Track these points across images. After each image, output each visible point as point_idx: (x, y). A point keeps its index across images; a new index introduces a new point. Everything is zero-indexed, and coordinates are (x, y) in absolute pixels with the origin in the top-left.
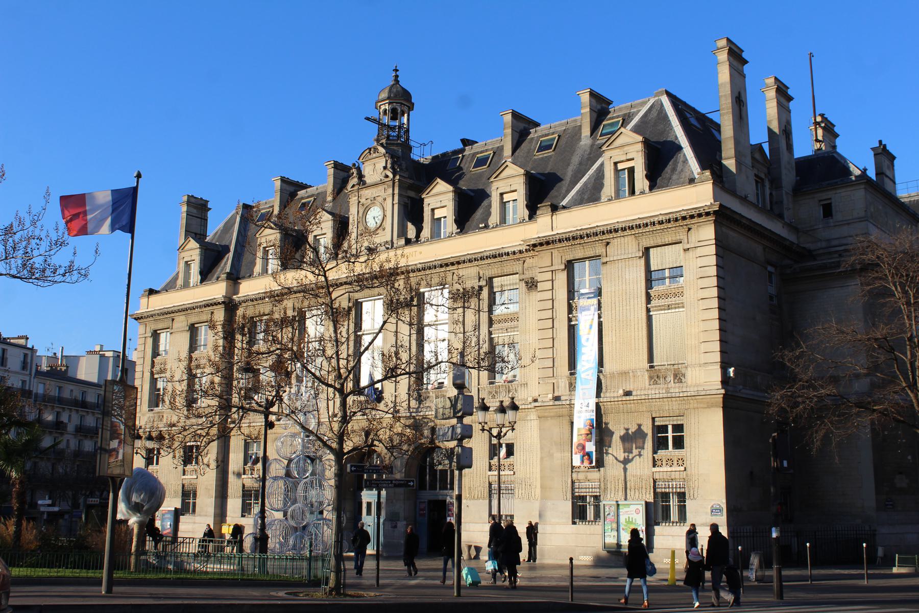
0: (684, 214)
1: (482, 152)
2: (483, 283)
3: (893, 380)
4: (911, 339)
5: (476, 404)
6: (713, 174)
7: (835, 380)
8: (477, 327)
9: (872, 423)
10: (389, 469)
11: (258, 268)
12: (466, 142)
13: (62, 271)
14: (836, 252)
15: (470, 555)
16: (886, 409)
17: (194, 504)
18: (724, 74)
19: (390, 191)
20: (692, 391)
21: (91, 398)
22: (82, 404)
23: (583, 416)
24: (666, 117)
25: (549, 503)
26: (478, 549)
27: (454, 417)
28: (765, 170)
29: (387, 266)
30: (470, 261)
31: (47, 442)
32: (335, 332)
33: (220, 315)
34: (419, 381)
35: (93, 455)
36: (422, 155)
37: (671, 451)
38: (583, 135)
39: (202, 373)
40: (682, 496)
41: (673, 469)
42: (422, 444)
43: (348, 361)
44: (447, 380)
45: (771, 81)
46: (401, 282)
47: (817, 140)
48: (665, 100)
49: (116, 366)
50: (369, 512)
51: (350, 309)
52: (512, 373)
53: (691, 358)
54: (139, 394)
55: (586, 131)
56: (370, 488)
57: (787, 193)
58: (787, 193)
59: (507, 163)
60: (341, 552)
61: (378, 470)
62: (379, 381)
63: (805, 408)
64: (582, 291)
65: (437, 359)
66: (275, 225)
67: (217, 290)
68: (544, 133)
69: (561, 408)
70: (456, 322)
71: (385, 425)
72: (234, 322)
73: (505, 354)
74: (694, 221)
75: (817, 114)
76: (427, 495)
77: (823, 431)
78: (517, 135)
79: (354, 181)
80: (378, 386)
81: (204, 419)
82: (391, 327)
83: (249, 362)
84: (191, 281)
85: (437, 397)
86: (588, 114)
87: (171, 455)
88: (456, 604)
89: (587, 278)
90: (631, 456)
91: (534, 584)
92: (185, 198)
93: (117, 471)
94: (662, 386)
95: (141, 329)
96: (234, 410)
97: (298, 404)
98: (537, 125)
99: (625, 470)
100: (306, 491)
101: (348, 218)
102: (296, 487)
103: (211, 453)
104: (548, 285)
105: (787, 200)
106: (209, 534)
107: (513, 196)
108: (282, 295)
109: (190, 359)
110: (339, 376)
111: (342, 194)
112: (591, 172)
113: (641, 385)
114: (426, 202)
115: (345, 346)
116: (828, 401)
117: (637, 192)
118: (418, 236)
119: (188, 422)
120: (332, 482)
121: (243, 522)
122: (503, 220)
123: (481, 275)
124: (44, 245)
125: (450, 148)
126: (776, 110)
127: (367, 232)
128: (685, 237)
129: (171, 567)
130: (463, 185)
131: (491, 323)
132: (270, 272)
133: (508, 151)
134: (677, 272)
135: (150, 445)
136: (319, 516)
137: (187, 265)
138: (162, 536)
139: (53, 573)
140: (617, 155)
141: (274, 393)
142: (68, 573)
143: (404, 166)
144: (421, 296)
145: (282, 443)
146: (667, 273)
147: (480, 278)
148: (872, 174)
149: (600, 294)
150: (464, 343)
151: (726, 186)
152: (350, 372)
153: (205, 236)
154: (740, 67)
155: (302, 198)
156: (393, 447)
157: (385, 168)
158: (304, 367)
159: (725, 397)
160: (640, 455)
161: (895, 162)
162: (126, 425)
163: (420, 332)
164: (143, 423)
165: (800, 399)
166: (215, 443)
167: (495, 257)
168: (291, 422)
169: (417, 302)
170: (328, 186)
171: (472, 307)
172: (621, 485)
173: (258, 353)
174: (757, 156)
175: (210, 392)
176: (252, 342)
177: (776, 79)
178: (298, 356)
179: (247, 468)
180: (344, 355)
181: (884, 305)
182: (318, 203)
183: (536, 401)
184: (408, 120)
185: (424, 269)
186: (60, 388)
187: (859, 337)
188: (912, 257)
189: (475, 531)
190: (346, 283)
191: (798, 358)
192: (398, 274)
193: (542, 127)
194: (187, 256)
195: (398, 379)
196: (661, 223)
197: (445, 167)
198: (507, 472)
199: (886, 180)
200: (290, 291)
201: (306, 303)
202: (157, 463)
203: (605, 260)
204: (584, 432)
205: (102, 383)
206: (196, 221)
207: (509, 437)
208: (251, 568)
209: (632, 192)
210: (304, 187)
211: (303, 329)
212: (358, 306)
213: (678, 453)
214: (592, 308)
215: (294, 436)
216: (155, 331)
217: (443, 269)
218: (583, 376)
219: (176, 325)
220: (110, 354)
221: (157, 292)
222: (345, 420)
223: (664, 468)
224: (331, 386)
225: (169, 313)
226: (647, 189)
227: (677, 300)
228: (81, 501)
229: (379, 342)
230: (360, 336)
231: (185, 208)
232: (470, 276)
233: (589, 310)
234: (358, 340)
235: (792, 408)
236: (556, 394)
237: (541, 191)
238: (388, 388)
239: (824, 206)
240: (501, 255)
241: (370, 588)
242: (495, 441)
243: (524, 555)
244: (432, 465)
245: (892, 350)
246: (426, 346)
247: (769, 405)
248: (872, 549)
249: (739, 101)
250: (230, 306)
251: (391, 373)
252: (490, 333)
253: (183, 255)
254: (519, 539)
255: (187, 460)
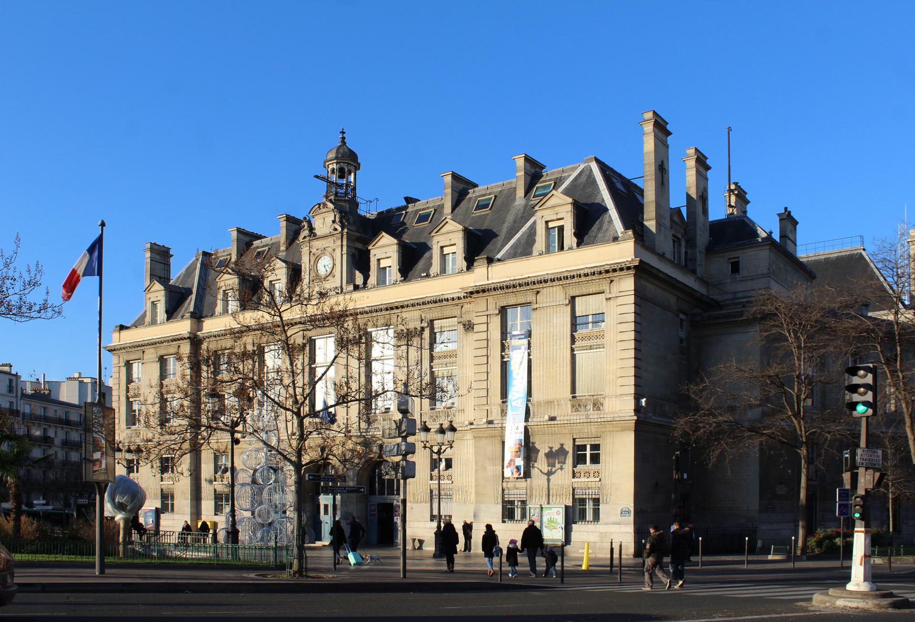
0: (607, 268)
1: (423, 209)
2: (425, 324)
3: (781, 409)
4: (799, 377)
5: (418, 426)
6: (635, 233)
7: (732, 409)
8: (419, 362)
9: (761, 444)
10: (343, 478)
11: (219, 308)
12: (409, 200)
13: (37, 308)
14: (740, 303)
15: (414, 546)
16: (773, 433)
17: (173, 505)
18: (649, 144)
19: (339, 242)
20: (609, 417)
21: (74, 417)
22: (67, 422)
23: (514, 436)
24: (594, 182)
25: (483, 506)
26: (421, 542)
27: (399, 436)
28: (682, 231)
29: (336, 309)
30: (413, 305)
31: (37, 453)
32: (291, 364)
33: (186, 348)
34: (368, 406)
35: (78, 465)
36: (369, 210)
37: (588, 466)
38: (517, 196)
39: (173, 398)
40: (597, 501)
41: (590, 480)
42: (371, 458)
43: (304, 389)
44: (393, 406)
45: (691, 151)
46: (350, 323)
47: (730, 206)
48: (594, 167)
49: (94, 390)
50: (326, 512)
51: (304, 345)
52: (451, 401)
53: (608, 390)
54: (117, 415)
55: (520, 193)
56: (326, 493)
57: (700, 252)
58: (700, 252)
59: (447, 220)
60: (304, 542)
61: (333, 479)
62: (332, 406)
63: (705, 432)
64: (514, 333)
65: (383, 389)
66: (233, 270)
67: (183, 327)
68: (481, 193)
69: (493, 430)
70: (400, 358)
71: (337, 442)
72: (198, 354)
73: (445, 385)
74: (616, 274)
75: (732, 181)
76: (377, 499)
77: (717, 452)
78: (456, 195)
79: (305, 233)
80: (332, 410)
81: (176, 436)
82: (342, 361)
83: (214, 388)
84: (158, 318)
85: (384, 420)
86: (523, 177)
87: (149, 465)
88: (402, 584)
89: (519, 322)
90: (554, 470)
91: (468, 569)
92: (149, 246)
93: (102, 478)
94: (582, 413)
95: (115, 360)
96: (203, 428)
97: (260, 424)
98: (475, 186)
99: (549, 480)
100: (270, 494)
101: (301, 266)
102: (262, 492)
103: (185, 464)
104: (484, 327)
105: (700, 258)
106: (187, 528)
107: (453, 249)
108: (242, 332)
109: (161, 386)
110: (296, 402)
111: (294, 244)
112: (524, 229)
113: (564, 412)
114: (372, 253)
115: (300, 376)
116: (725, 426)
117: (566, 247)
118: (365, 283)
119: (162, 438)
120: (293, 488)
121: (216, 519)
122: (443, 270)
124: (18, 286)
125: (394, 205)
126: (694, 178)
127: (318, 278)
128: (608, 288)
129: (155, 554)
130: (407, 238)
131: (432, 358)
132: (230, 312)
133: (448, 208)
134: (599, 318)
135: (129, 456)
136: (283, 515)
137: (154, 304)
138: (145, 530)
139: (52, 558)
140: (548, 215)
141: (238, 415)
142: (65, 558)
143: (351, 220)
144: (368, 335)
145: (248, 456)
146: (590, 319)
147: (422, 320)
148: (776, 236)
149: (530, 336)
150: (408, 375)
151: (647, 244)
152: (305, 399)
153: (168, 279)
154: (664, 138)
155: (258, 247)
156: (346, 460)
157: (334, 222)
158: (264, 394)
159: (638, 424)
160: (562, 469)
161: (798, 226)
162: (106, 441)
163: (368, 366)
164: (121, 439)
165: (701, 425)
166: (188, 456)
167: (435, 302)
168: (254, 439)
169: (364, 340)
170: (281, 235)
171: (415, 344)
172: (545, 492)
173: (222, 382)
174: (676, 218)
175: (181, 414)
176: (216, 372)
177: (696, 149)
178: (258, 385)
179: (217, 476)
180: (299, 383)
181: (778, 348)
182: (272, 252)
183: (471, 424)
184: (355, 178)
185: (371, 312)
186: (45, 408)
187: (755, 374)
188: (806, 308)
189: (419, 527)
190: (300, 323)
191: (701, 391)
192: (347, 316)
193: (480, 188)
194: (153, 297)
195: (349, 404)
196: (586, 275)
197: (388, 222)
198: (446, 481)
199: (789, 242)
200: (249, 329)
201: (264, 339)
202: (137, 471)
203: (535, 306)
204: (514, 449)
205: (83, 404)
206: (159, 267)
207: (448, 453)
208: (225, 555)
209: (561, 248)
210: (259, 237)
211: (262, 362)
212: (312, 342)
213: (595, 467)
214: (523, 348)
215: (258, 450)
216: (128, 362)
217: (388, 312)
218: (513, 404)
219: (146, 356)
220: (89, 380)
221: (127, 328)
222: (302, 438)
223: (582, 479)
224: (289, 410)
225: (140, 346)
226: (575, 245)
227: (599, 341)
228: (72, 501)
229: (331, 373)
230: (315, 368)
231: (148, 255)
232: (412, 318)
233: (520, 349)
234: (312, 372)
235: (694, 431)
236: (490, 419)
237: (478, 246)
238: (341, 412)
239: (732, 263)
240: (441, 301)
241: (328, 571)
242: (435, 456)
243: (460, 546)
244: (380, 475)
245: (782, 385)
246: (374, 377)
247: (675, 429)
248: (752, 542)
249: (662, 169)
250: (195, 341)
251: (343, 400)
252: (431, 367)
253: (149, 295)
254: (457, 534)
255: (164, 470)
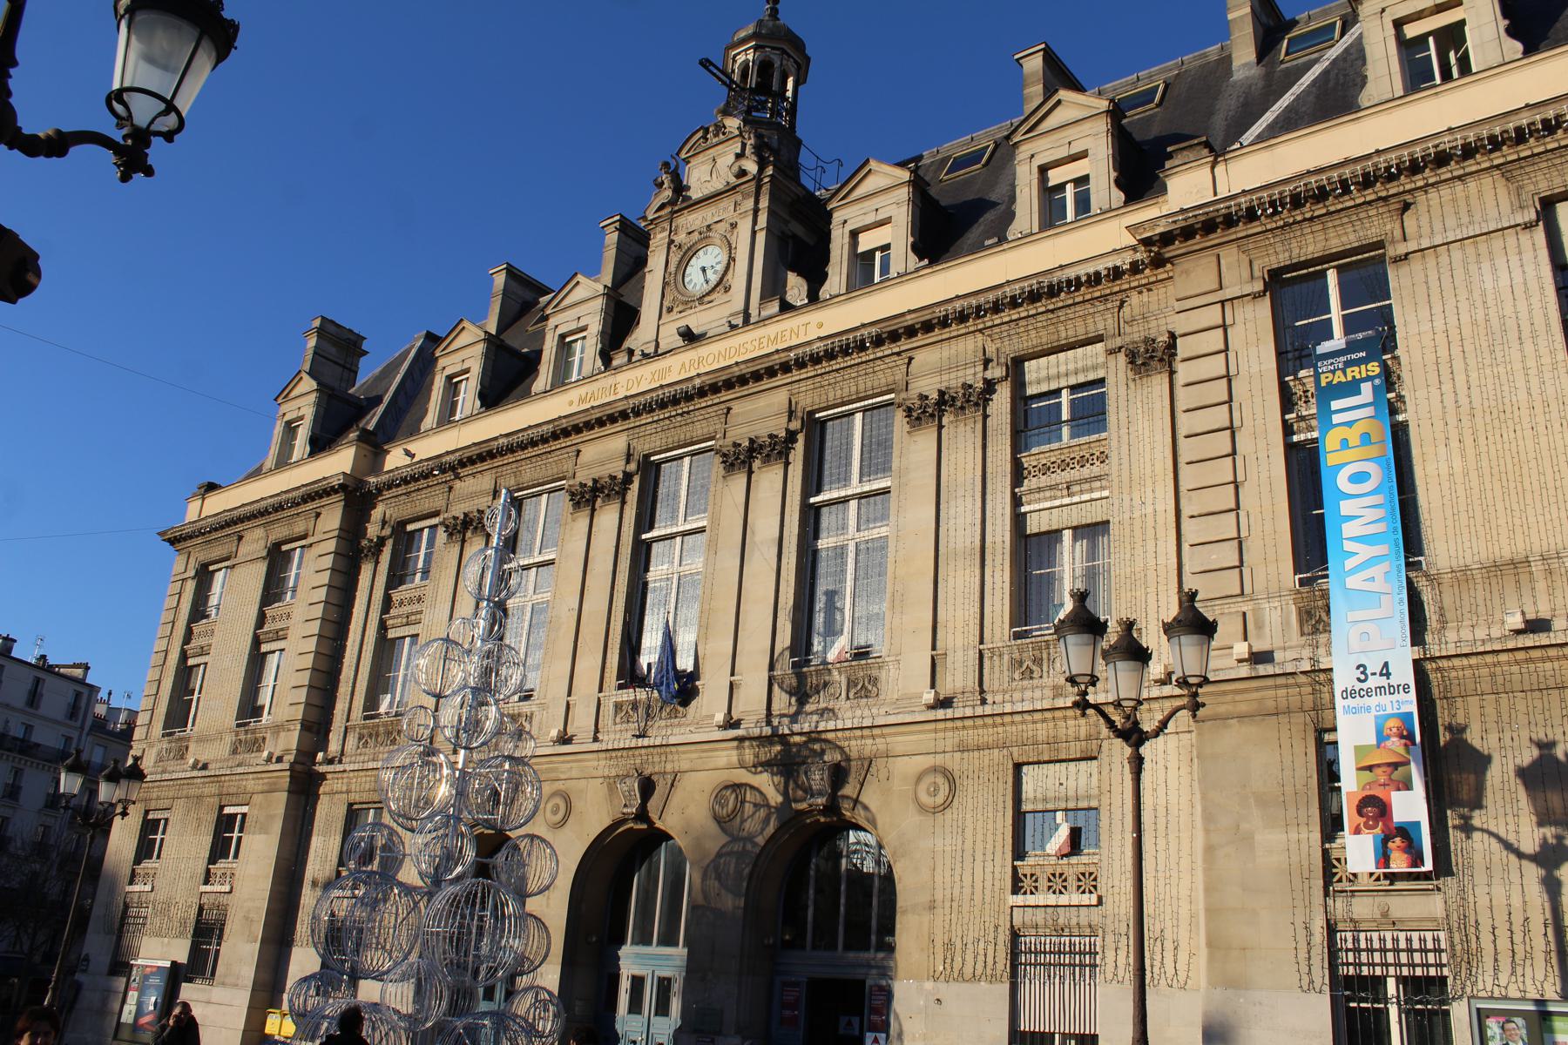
2: (996, 372)
19: (750, 203)
123: (991, 349)
147: (986, 363)
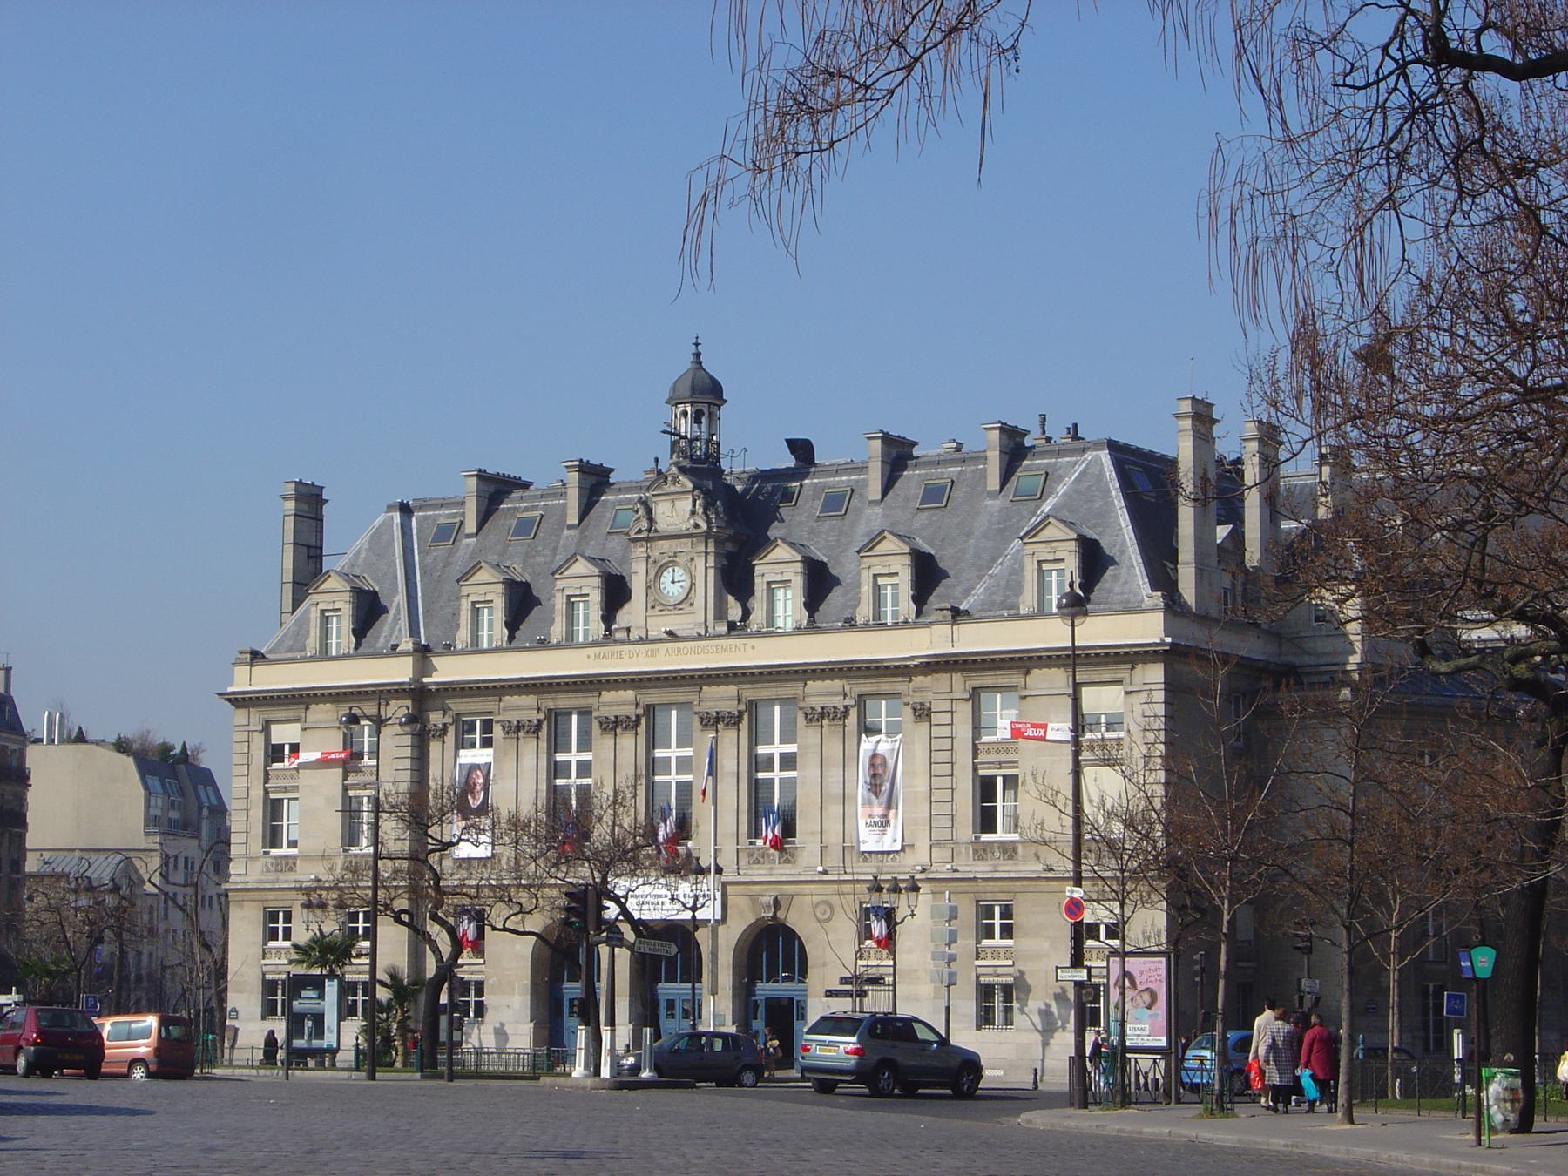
157: (693, 513)
